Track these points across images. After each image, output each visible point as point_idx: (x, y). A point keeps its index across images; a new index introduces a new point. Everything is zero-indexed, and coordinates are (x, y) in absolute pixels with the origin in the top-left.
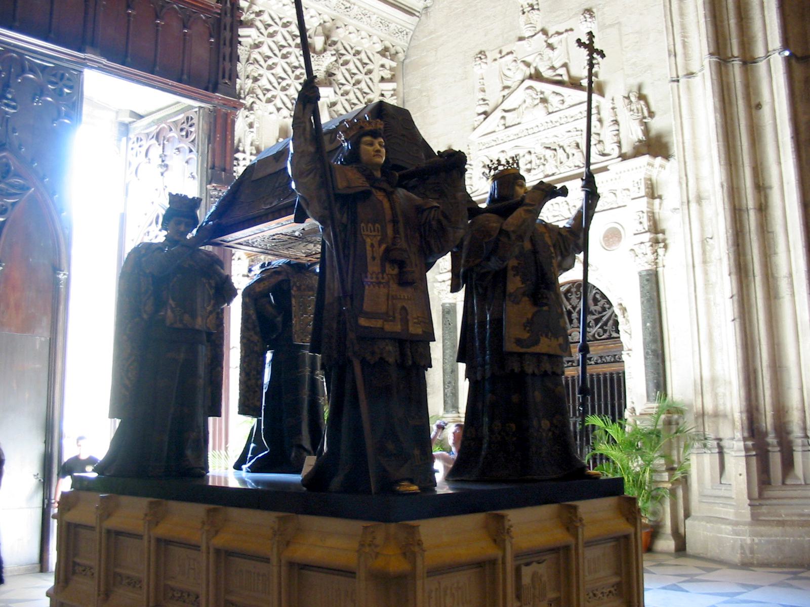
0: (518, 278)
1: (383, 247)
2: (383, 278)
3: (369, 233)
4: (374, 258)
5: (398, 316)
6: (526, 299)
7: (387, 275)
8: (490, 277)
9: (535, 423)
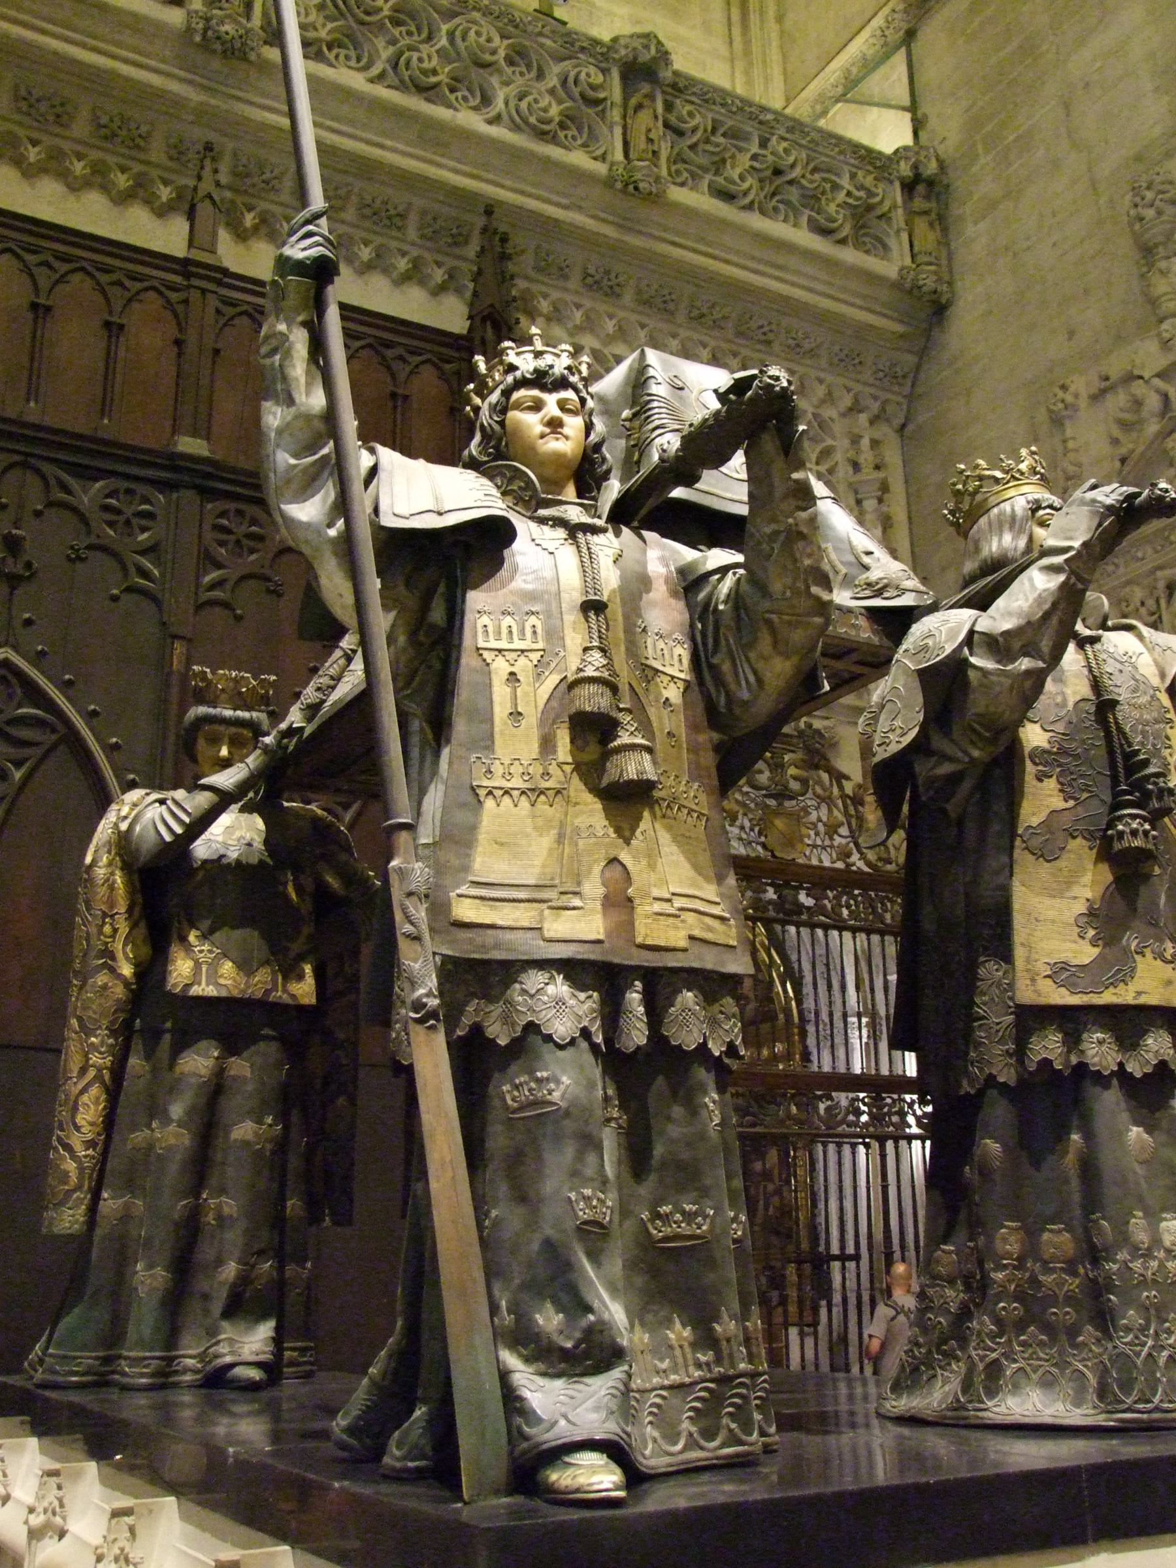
0: (1051, 784)
1: (552, 680)
2: (546, 774)
3: (503, 644)
4: (516, 715)
5: (593, 888)
6: (1078, 844)
7: (559, 765)
8: (967, 786)
9: (1138, 1228)
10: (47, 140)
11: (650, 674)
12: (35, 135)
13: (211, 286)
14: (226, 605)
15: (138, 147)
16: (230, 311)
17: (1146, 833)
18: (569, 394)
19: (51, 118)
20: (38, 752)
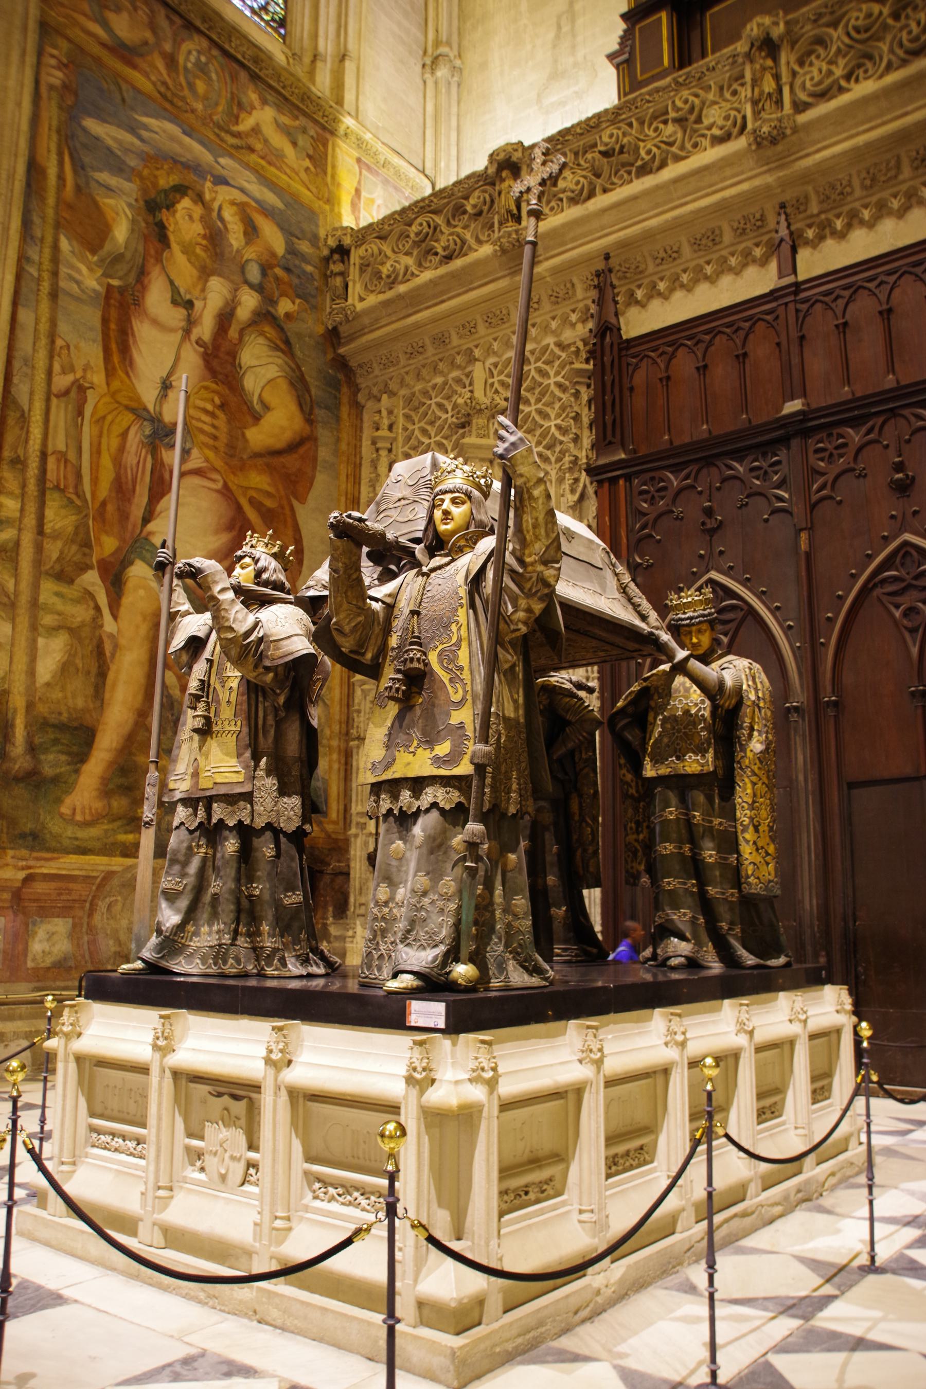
10: (715, 256)
11: (223, 681)
12: (707, 258)
13: (792, 298)
14: (829, 498)
15: (759, 227)
16: (804, 307)
17: (391, 688)
18: (247, 560)
19: (710, 244)
20: (733, 626)
